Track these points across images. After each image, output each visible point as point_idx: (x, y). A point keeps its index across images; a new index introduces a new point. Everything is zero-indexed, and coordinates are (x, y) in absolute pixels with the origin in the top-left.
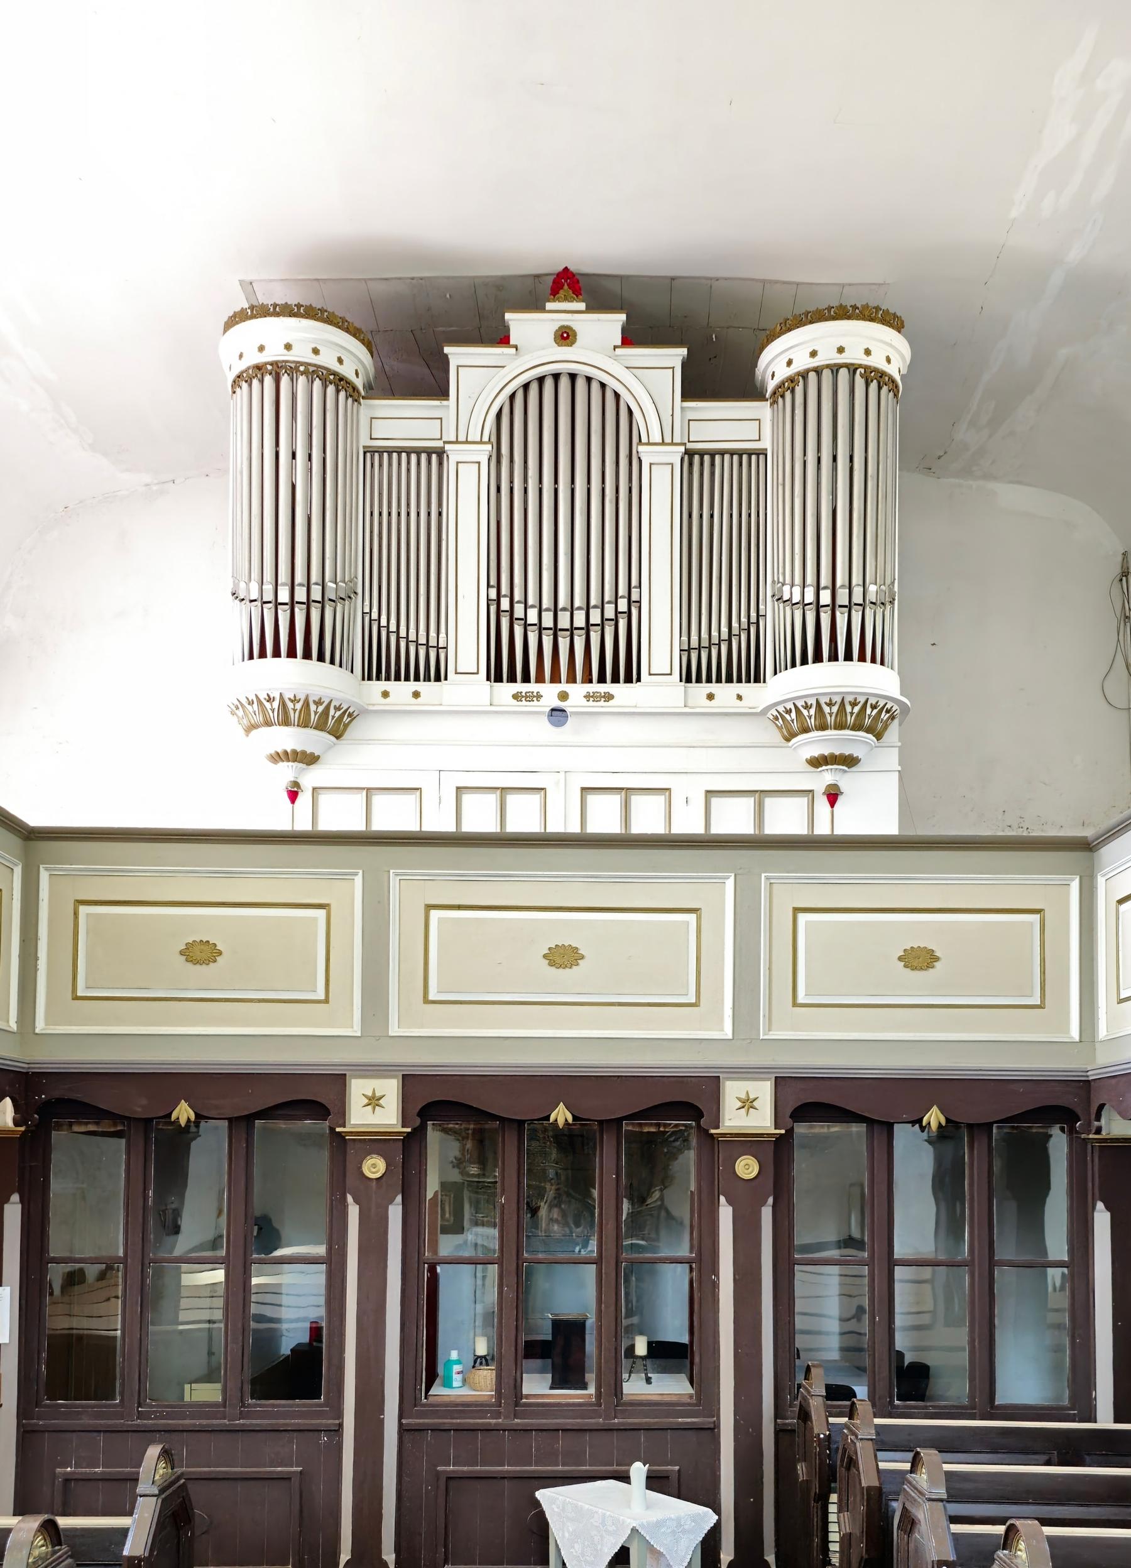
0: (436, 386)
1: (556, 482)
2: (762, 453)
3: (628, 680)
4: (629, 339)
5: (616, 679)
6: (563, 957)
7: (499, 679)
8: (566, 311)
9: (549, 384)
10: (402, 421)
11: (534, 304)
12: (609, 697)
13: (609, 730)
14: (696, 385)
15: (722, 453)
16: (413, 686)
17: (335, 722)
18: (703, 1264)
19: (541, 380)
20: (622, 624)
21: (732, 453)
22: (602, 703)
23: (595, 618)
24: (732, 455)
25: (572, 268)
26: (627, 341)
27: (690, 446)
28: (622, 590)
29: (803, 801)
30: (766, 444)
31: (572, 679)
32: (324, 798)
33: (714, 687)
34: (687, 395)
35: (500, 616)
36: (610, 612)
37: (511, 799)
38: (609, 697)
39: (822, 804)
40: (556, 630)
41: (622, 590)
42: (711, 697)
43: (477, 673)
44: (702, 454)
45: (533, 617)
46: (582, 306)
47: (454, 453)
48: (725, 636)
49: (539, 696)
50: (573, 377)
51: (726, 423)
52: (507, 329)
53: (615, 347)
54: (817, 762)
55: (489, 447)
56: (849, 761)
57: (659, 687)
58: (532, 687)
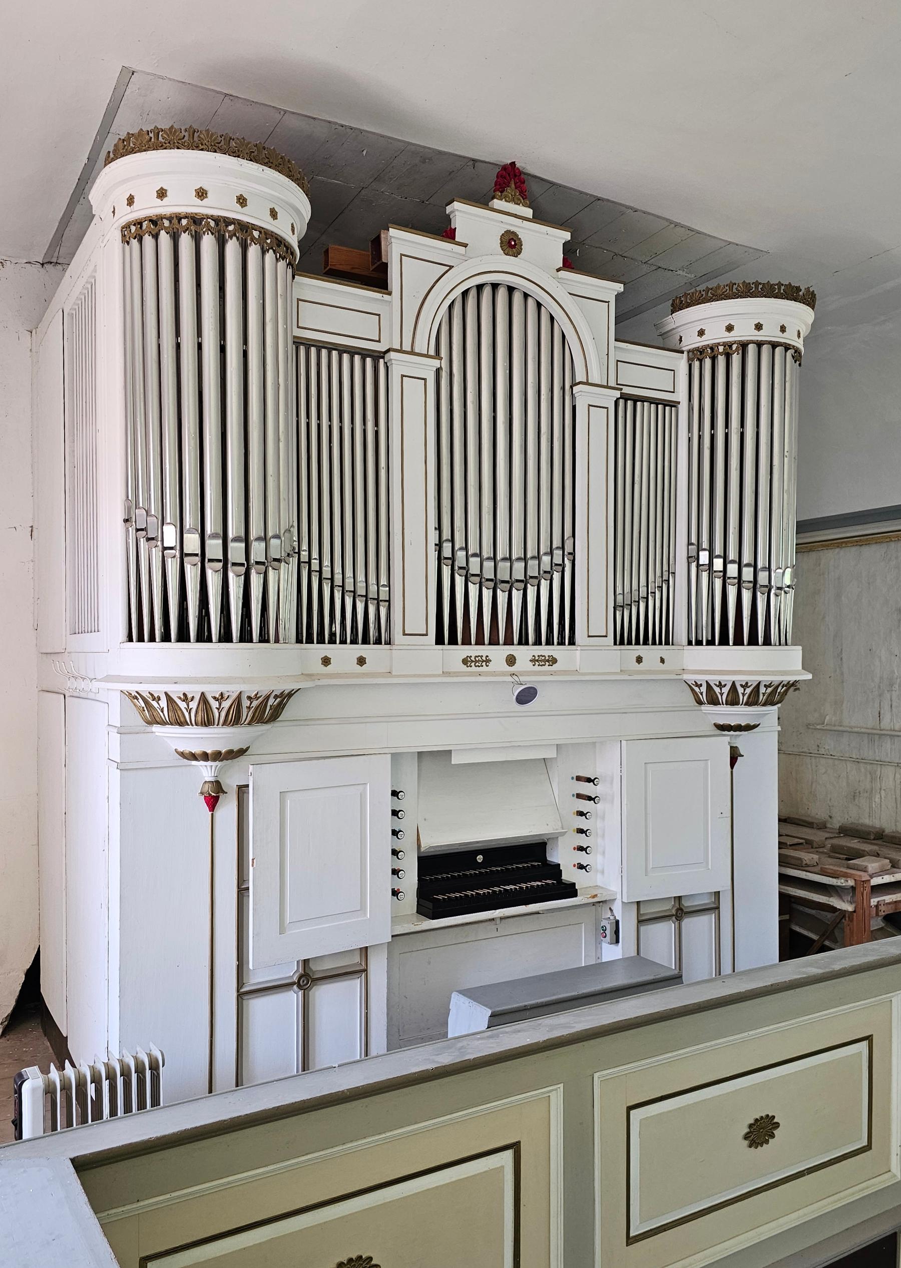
0: (375, 277)
1: (727, 435)
2: (674, 405)
4: (573, 260)
5: (561, 643)
8: (509, 216)
9: (487, 292)
11: (482, 201)
15: (643, 399)
19: (480, 288)
22: (546, 668)
24: (657, 404)
25: (518, 165)
38: (553, 661)
43: (426, 635)
46: (528, 212)
47: (399, 364)
48: (643, 593)
49: (488, 661)
50: (511, 290)
52: (448, 219)
55: (436, 363)
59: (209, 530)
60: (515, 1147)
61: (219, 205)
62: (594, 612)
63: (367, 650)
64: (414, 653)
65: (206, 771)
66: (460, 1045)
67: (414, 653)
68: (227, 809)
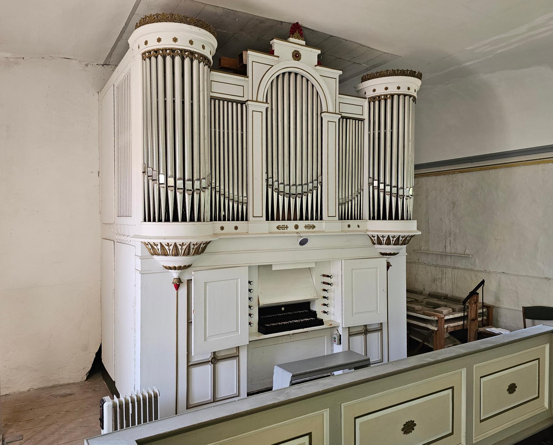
0: (241, 70)
2: (362, 120)
4: (321, 62)
5: (317, 219)
8: (296, 44)
9: (286, 76)
10: (226, 84)
11: (285, 38)
15: (350, 118)
16: (236, 223)
19: (284, 74)
22: (311, 230)
25: (299, 23)
26: (320, 63)
27: (343, 115)
31: (301, 219)
38: (314, 227)
46: (304, 43)
47: (252, 106)
48: (350, 198)
49: (287, 227)
50: (296, 74)
51: (357, 107)
53: (316, 66)
55: (266, 105)
59: (178, 177)
60: (310, 434)
61: (182, 44)
62: (330, 207)
64: (258, 224)
65: (175, 274)
66: (286, 392)
67: (258, 224)
68: (183, 290)
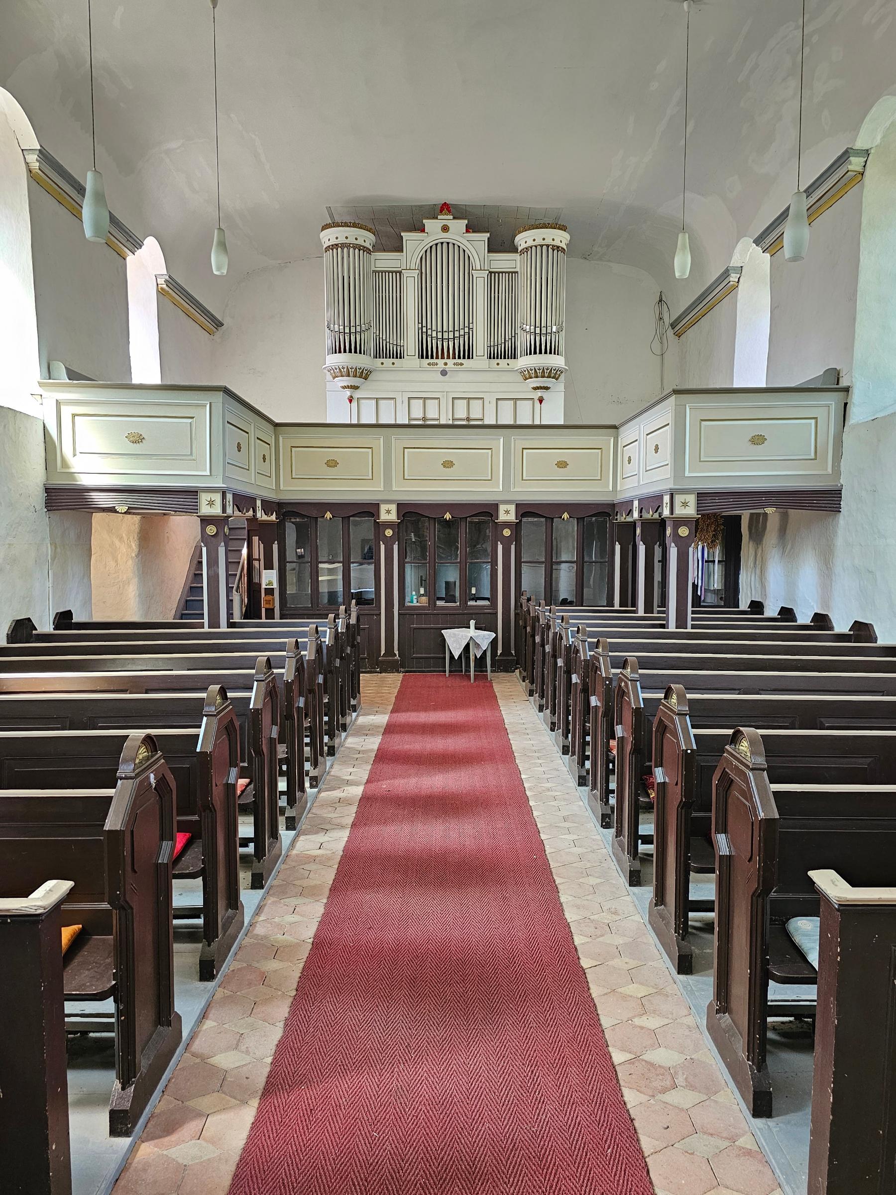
3: (469, 358)
5: (464, 358)
6: (448, 464)
7: (422, 357)
8: (445, 219)
9: (439, 246)
10: (386, 261)
12: (462, 364)
13: (462, 376)
14: (494, 247)
15: (502, 273)
16: (392, 360)
17: (364, 374)
18: (494, 563)
19: (436, 245)
20: (466, 337)
21: (506, 273)
23: (457, 334)
26: (467, 231)
28: (466, 325)
29: (531, 402)
30: (518, 269)
31: (448, 357)
32: (362, 401)
33: (499, 361)
34: (489, 252)
35: (423, 332)
36: (462, 332)
37: (428, 401)
38: (462, 364)
39: (537, 403)
40: (443, 339)
41: (466, 325)
42: (498, 364)
44: (495, 273)
45: (434, 334)
50: (448, 243)
51: (503, 261)
54: (535, 389)
56: (547, 388)
57: (480, 361)
58: (434, 361)
63: (395, 360)
